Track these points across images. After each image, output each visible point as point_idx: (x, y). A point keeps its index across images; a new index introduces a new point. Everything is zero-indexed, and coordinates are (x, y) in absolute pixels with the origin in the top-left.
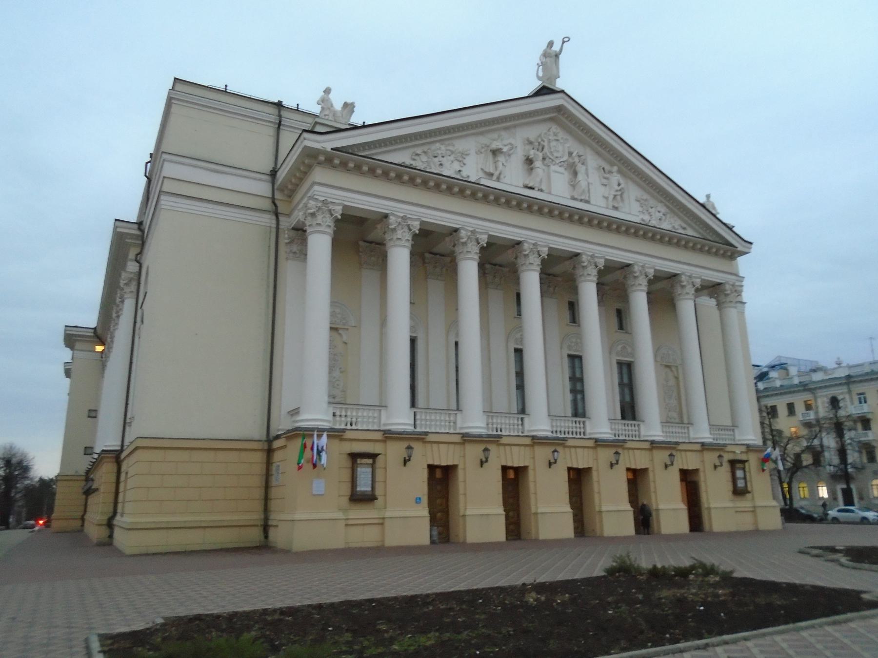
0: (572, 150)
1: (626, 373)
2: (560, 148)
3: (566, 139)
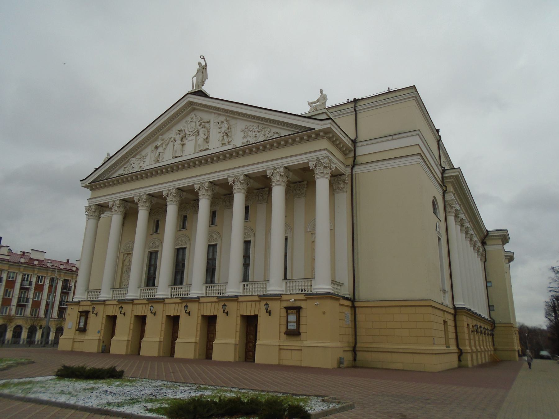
1: (152, 258)
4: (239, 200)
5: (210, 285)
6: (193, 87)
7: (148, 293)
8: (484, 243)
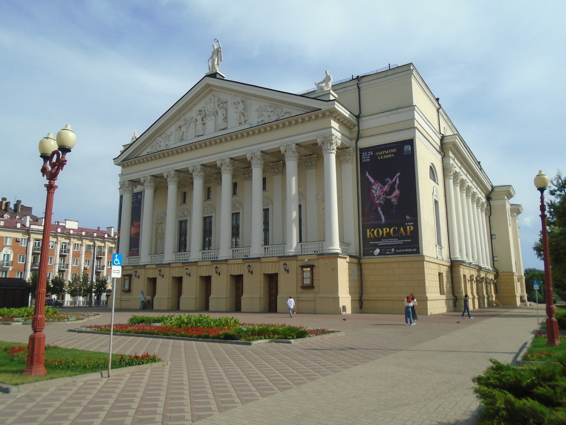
4: (257, 173)
5: (236, 249)
6: (210, 69)
7: (183, 256)
8: (488, 198)
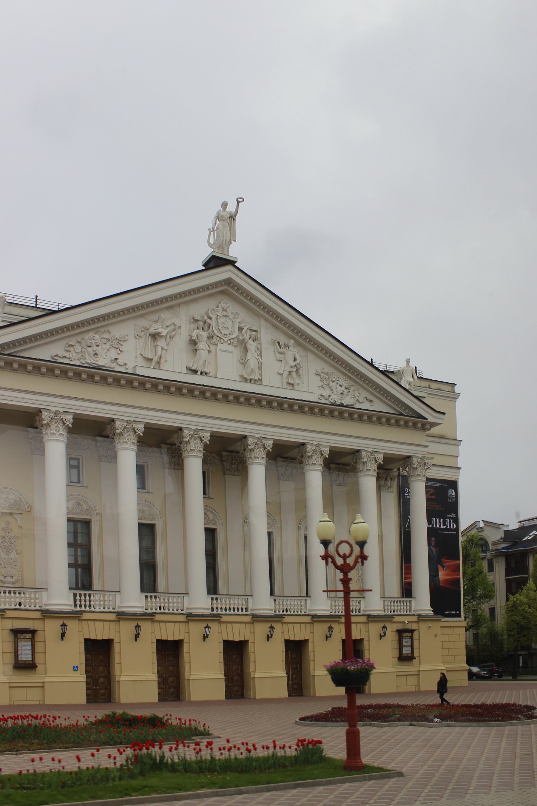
0: (242, 325)
2: (229, 324)
3: (237, 314)
5: (153, 595)
